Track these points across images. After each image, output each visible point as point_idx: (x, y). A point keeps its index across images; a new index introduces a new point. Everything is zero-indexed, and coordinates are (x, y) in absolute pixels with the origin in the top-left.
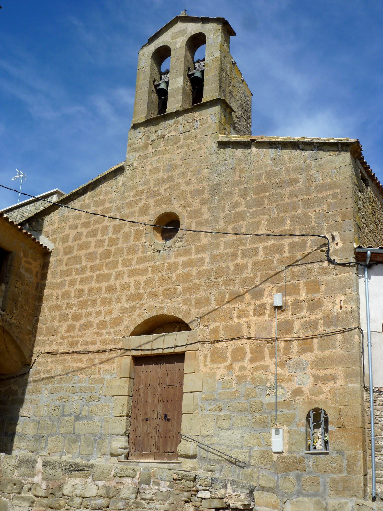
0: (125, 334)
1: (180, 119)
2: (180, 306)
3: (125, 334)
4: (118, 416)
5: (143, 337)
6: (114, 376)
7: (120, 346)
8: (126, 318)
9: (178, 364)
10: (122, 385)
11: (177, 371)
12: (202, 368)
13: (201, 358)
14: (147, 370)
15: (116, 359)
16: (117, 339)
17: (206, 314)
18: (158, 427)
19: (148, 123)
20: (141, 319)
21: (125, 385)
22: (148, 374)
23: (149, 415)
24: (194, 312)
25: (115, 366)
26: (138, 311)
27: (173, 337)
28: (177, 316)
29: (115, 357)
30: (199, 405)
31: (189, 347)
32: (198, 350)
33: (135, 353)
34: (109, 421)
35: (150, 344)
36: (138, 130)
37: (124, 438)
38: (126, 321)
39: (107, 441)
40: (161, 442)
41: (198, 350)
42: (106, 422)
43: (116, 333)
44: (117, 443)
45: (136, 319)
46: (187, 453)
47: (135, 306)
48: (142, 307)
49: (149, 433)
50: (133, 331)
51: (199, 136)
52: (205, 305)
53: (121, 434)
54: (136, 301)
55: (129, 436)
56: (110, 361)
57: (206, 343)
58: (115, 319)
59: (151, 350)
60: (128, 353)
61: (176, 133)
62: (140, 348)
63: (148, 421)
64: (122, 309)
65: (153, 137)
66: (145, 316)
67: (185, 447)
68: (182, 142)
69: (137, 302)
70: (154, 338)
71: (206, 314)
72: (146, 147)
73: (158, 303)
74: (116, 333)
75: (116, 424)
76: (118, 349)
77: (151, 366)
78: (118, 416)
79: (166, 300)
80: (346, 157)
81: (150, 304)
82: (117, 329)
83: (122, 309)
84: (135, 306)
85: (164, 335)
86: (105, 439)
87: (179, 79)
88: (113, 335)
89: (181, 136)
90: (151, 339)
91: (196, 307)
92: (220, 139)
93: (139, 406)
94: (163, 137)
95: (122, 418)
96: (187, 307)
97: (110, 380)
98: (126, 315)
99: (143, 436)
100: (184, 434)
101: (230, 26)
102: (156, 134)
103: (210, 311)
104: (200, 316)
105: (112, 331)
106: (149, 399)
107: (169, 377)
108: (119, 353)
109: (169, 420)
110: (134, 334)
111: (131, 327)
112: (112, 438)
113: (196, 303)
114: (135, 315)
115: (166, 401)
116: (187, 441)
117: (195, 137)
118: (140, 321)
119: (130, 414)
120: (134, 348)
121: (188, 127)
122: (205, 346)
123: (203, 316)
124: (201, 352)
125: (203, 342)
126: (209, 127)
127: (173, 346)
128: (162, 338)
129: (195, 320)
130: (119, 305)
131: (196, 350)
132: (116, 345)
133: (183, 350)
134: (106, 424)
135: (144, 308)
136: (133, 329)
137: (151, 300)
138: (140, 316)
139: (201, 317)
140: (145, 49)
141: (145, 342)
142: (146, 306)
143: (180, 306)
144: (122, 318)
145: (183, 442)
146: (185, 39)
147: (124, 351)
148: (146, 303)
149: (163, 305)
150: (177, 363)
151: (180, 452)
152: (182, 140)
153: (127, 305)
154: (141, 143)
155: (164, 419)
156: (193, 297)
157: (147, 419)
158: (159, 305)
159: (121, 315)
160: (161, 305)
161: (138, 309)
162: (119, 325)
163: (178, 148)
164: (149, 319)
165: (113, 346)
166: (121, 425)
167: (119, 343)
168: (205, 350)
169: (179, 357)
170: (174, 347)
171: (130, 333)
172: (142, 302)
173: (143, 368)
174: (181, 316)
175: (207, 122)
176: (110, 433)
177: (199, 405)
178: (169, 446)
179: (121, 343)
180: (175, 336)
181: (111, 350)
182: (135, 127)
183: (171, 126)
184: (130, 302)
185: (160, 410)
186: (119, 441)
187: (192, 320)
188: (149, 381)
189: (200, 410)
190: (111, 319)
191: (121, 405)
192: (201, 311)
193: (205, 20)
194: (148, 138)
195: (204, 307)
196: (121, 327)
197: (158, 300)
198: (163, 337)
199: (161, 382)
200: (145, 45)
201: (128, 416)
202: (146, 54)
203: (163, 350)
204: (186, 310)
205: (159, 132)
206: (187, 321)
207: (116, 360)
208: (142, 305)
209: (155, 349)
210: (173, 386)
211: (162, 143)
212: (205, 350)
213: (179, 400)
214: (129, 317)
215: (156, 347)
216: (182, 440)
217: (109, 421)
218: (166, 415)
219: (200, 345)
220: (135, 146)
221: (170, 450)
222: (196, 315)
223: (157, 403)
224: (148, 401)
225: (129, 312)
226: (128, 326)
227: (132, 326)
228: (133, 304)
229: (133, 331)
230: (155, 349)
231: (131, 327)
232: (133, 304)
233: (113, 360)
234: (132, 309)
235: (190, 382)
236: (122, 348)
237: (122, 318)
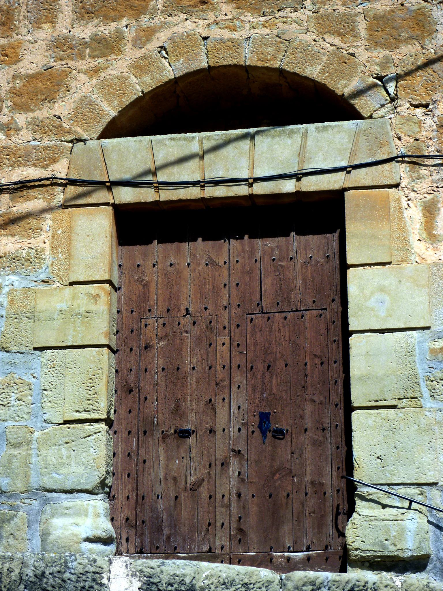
0: (79, 129)
2: (309, 38)
3: (79, 129)
4: (66, 422)
5: (159, 142)
6: (43, 277)
7: (61, 169)
8: (82, 77)
9: (302, 238)
10: (82, 309)
11: (299, 261)
12: (419, 248)
13: (414, 215)
14: (172, 260)
15: (48, 216)
16: (46, 148)
17: (419, 68)
18: (235, 462)
20: (147, 79)
21: (92, 307)
22: (179, 273)
23: (192, 417)
24: (369, 59)
25: (42, 242)
26: (131, 54)
27: (289, 141)
28: (297, 70)
29: (44, 211)
30: (421, 375)
31: (361, 177)
32: (397, 186)
33: (126, 195)
34: (28, 443)
35: (194, 163)
37: (99, 504)
38: (82, 86)
39: (21, 514)
41: (397, 186)
42: (15, 446)
43: (39, 127)
44: (71, 520)
45: (123, 79)
46: (392, 550)
47: (119, 36)
48: (148, 39)
49: (195, 487)
50: (113, 121)
52: (411, 38)
53: (88, 487)
54: (121, 17)
55: (111, 497)
56: (22, 223)
57: (427, 162)
58: (31, 78)
59: (202, 184)
60: (102, 196)
62: (150, 178)
63: (191, 441)
64: (61, 46)
66: (161, 69)
67: (367, 528)
69: (124, 21)
70: (207, 145)
71: (419, 68)
73: (213, 27)
74: (39, 127)
75: (64, 452)
76: (53, 182)
77: (187, 246)
78: (66, 422)
79: (248, 17)
81: (179, 29)
82: (44, 113)
83: (61, 46)
84: (119, 36)
85: (252, 137)
86: (14, 508)
88: (26, 135)
90: (195, 148)
91: (374, 43)
93: (146, 386)
95: (88, 427)
96: (337, 41)
97: (26, 290)
98: (82, 64)
99: (172, 495)
100: (366, 481)
103: (432, 56)
104: (393, 71)
105: (21, 119)
106: (190, 360)
107: (268, 283)
108: (59, 196)
109: (279, 434)
110: (113, 130)
111: (105, 105)
112: (46, 502)
113: (370, 29)
114: (119, 66)
115: (260, 366)
116: (384, 506)
118: (139, 86)
119: (112, 416)
120: (127, 176)
122: (423, 172)
123: (408, 74)
124: (412, 195)
125: (415, 160)
127: (293, 169)
128: (246, 144)
129: (375, 85)
130: (46, 32)
131: (390, 186)
132: (45, 167)
133: (337, 186)
134: (15, 452)
135: (153, 45)
136: (114, 113)
137: (182, 16)
138: (140, 67)
139: (398, 78)
141: (172, 159)
142: (163, 37)
143: (309, 38)
144: (64, 74)
147: (80, 189)
148: (163, 26)
149: (235, 35)
150: (298, 234)
151: (363, 546)
153: (85, 32)
155: (258, 433)
156: (359, 9)
157: (185, 434)
158: (215, 33)
159: (58, 66)
160: (227, 34)
161: (129, 46)
162: (50, 98)
164: (176, 81)
165: (32, 173)
166: (91, 455)
167: (54, 161)
168: (424, 186)
169: (321, 214)
170: (298, 176)
171: (100, 128)
172: (146, 21)
173: (157, 253)
174: (314, 72)
176: (35, 485)
177: (421, 375)
178: (286, 529)
179: (65, 162)
180: (298, 138)
181: (23, 186)
184: (95, 21)
185: (238, 399)
186: (83, 513)
187: (362, 86)
188: (183, 296)
189: (426, 393)
190: (14, 77)
191: (86, 380)
192: (396, 56)
195: (406, 41)
196: (63, 107)
197: (211, 16)
198: (248, 141)
199: (236, 301)
201: (109, 422)
203: (251, 185)
204: (333, 53)
206: (344, 87)
207: (48, 222)
208: (149, 33)
209: (217, 183)
210: (290, 315)
212: (424, 186)
213: (317, 361)
214: (96, 71)
215: (221, 174)
216: (359, 504)
217: (28, 443)
218: (264, 417)
219: (401, 171)
221: (295, 542)
222: (376, 69)
223: (221, 374)
224: (187, 368)
225: (93, 57)
226: (91, 103)
227: (110, 103)
228: (108, 29)
229: (114, 119)
230: (217, 183)
231: (105, 105)
232: (108, 29)
233: (33, 222)
234: (106, 46)
235: (368, 295)
236: (71, 177)
237: (64, 74)
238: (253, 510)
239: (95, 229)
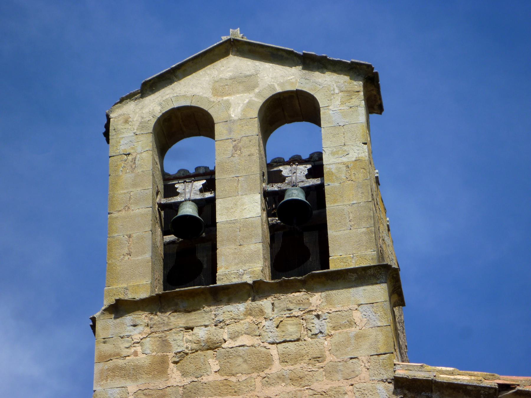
1: (266, 303)
36: (128, 319)
51: (330, 358)
61: (256, 341)
65: (181, 342)
68: (276, 368)
72: (160, 367)
87: (246, 199)
89: (274, 350)
92: (401, 373)
94: (213, 346)
101: (378, 87)
102: (188, 336)
117: (318, 359)
121: (292, 329)
126: (358, 337)
140: (130, 108)
152: (277, 362)
154: (144, 354)
163: (268, 382)
175: (351, 323)
182: (119, 308)
183: (236, 320)
193: (312, 62)
194: (165, 344)
200: (131, 97)
202: (136, 119)
205: (201, 333)
211: (214, 365)
220: (120, 362)
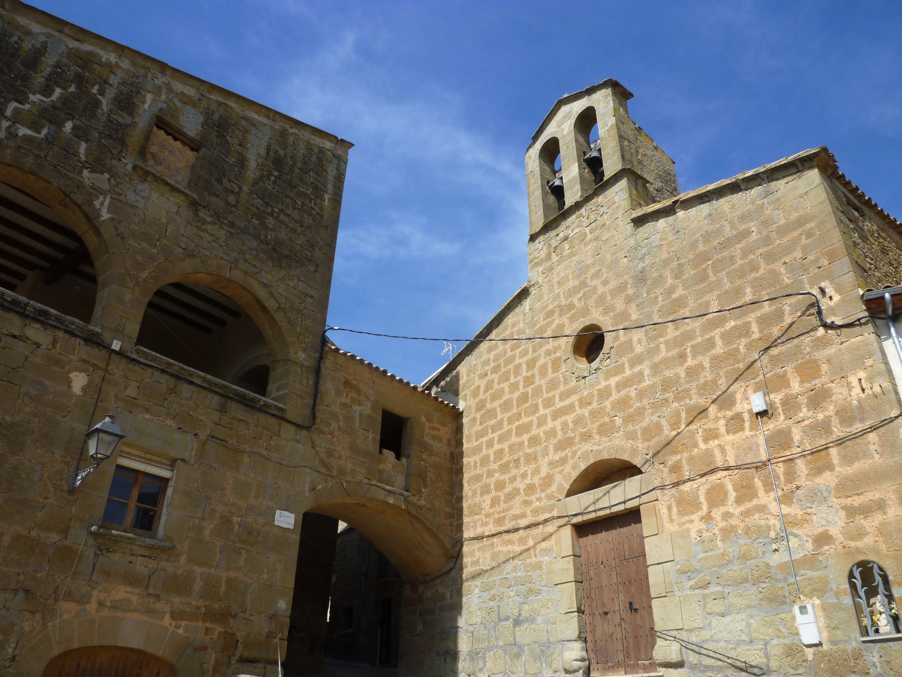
1: (583, 211)
2: (623, 443)
7: (555, 513)
11: (635, 535)
12: (667, 525)
13: (664, 511)
19: (548, 227)
26: (571, 462)
31: (645, 498)
36: (537, 241)
37: (578, 645)
38: (558, 479)
40: (631, 644)
42: (553, 624)
43: (549, 497)
47: (567, 456)
49: (612, 634)
51: (608, 223)
55: (585, 641)
58: (544, 478)
61: (581, 228)
64: (552, 464)
65: (554, 243)
67: (665, 650)
68: (589, 236)
72: (549, 257)
74: (549, 497)
77: (599, 535)
79: (604, 439)
80: (813, 176)
81: (584, 449)
82: (548, 492)
83: (552, 464)
87: (573, 168)
88: (545, 501)
89: (587, 230)
92: (634, 216)
93: (593, 595)
94: (566, 238)
95: (572, 615)
96: (631, 442)
98: (557, 470)
101: (621, 86)
102: (558, 238)
105: (543, 495)
107: (626, 547)
109: (636, 610)
110: (570, 494)
112: (563, 646)
113: (642, 434)
114: (568, 468)
115: (627, 582)
117: (603, 225)
118: (575, 475)
121: (593, 217)
122: (666, 492)
125: (662, 488)
126: (617, 208)
127: (623, 500)
130: (547, 460)
133: (637, 504)
136: (568, 487)
140: (531, 150)
142: (579, 453)
145: (660, 642)
146: (572, 121)
148: (579, 449)
149: (600, 447)
152: (589, 235)
153: (556, 458)
154: (543, 254)
157: (606, 613)
158: (595, 448)
159: (551, 472)
162: (550, 485)
163: (586, 245)
164: (586, 469)
165: (547, 516)
166: (571, 627)
169: (632, 516)
170: (624, 502)
172: (574, 448)
173: (592, 540)
174: (626, 457)
175: (614, 203)
178: (642, 651)
181: (546, 521)
182: (533, 238)
183: (573, 223)
185: (621, 597)
186: (573, 649)
193: (590, 91)
194: (550, 245)
195: (654, 437)
196: (553, 488)
197: (593, 441)
200: (530, 146)
202: (533, 155)
204: (632, 447)
205: (561, 235)
208: (575, 453)
209: (600, 510)
211: (567, 246)
212: (666, 498)
214: (561, 472)
216: (658, 639)
218: (631, 604)
220: (536, 261)
223: (615, 587)
230: (600, 510)
232: (563, 454)
234: (563, 461)
235: (654, 549)
238: (631, 644)
239: (567, 533)
